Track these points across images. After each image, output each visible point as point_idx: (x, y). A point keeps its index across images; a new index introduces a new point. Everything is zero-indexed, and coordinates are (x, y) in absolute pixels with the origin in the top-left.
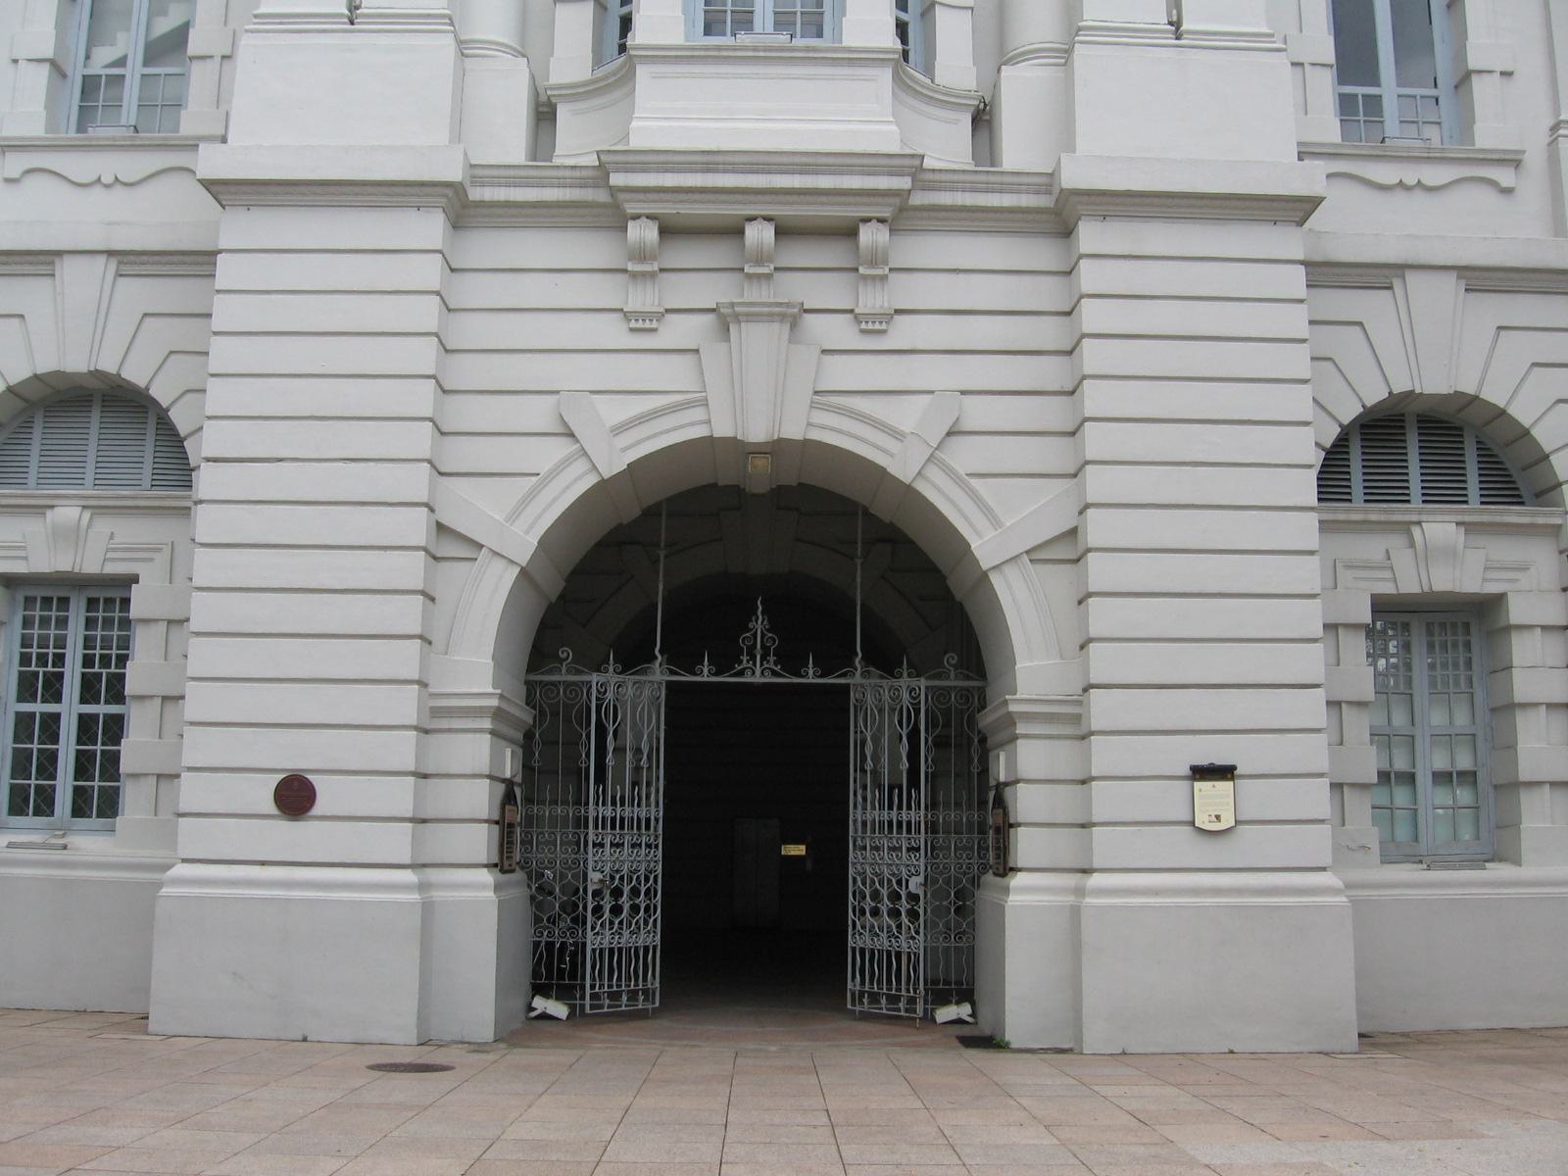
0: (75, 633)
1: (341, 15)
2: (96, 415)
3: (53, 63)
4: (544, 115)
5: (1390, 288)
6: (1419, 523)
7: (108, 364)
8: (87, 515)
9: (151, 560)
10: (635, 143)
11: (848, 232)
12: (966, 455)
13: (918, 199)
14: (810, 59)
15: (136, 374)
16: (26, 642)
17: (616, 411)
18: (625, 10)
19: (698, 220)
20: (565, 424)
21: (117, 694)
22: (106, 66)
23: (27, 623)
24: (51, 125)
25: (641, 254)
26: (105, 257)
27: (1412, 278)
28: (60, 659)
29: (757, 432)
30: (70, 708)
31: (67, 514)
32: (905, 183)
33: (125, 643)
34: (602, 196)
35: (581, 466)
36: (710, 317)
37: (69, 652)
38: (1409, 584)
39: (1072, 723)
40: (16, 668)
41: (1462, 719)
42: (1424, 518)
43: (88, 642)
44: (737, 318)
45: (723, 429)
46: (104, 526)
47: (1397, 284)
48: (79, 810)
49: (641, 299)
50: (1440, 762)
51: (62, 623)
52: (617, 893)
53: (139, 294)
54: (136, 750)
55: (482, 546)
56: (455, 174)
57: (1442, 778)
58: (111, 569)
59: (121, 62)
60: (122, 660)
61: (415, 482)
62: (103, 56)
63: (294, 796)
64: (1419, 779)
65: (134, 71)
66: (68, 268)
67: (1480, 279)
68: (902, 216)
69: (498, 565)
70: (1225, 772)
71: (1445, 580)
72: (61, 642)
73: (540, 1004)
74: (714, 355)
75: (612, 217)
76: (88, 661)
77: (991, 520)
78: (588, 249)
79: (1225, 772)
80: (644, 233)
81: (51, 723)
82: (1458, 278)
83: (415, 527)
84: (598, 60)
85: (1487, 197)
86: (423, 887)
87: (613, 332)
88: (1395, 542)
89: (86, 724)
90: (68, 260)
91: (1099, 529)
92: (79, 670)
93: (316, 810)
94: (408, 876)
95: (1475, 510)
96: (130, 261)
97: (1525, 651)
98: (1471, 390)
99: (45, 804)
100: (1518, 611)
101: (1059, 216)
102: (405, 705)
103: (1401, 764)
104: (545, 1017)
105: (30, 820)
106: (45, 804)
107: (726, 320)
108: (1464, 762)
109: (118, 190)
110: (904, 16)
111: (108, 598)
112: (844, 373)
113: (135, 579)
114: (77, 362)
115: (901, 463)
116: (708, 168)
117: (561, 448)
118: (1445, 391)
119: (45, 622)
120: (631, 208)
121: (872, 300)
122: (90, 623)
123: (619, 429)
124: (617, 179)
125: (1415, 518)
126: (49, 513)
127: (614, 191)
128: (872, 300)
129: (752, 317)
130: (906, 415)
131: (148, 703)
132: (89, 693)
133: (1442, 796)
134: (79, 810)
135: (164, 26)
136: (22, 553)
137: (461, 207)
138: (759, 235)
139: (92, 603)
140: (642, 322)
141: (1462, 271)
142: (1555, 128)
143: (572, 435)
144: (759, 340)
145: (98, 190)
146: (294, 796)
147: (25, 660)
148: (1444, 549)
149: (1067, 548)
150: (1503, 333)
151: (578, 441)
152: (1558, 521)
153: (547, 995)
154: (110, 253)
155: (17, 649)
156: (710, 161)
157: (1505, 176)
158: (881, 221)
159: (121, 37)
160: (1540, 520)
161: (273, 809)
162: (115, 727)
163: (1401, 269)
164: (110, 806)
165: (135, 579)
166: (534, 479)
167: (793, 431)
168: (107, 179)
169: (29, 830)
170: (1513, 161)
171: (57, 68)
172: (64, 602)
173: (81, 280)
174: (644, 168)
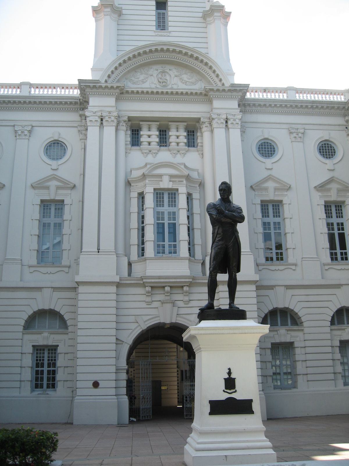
0: (46, 355)
1: (97, 251)
2: (48, 316)
3: (37, 250)
4: (130, 264)
5: (273, 289)
6: (279, 330)
7: (52, 308)
8: (49, 334)
9: (61, 342)
11: (182, 287)
13: (194, 281)
14: (175, 259)
15: (57, 309)
16: (37, 357)
17: (146, 318)
18: (143, 246)
19: (156, 286)
20: (136, 320)
21: (54, 365)
22: (44, 250)
23: (37, 353)
24: (38, 263)
25: (148, 292)
26: (51, 288)
27: (277, 287)
28: (43, 360)
29: (168, 321)
30: (46, 369)
31: (46, 334)
32: (191, 280)
33: (55, 357)
34: (141, 282)
35: (141, 329)
36: (160, 302)
37: (45, 359)
38: (278, 341)
40: (35, 362)
41: (288, 363)
42: (280, 329)
43: (49, 357)
44: (164, 303)
45: (162, 321)
46: (52, 336)
47: (274, 288)
48: (48, 387)
49: (149, 299)
50: (285, 371)
51: (44, 353)
52: (145, 399)
53: (58, 294)
54: (60, 376)
55: (123, 342)
56: (117, 279)
57: (285, 374)
58: (54, 344)
59: (48, 249)
60: (55, 360)
61: (114, 332)
62: (45, 247)
63: (96, 385)
64: (281, 374)
65: (51, 250)
66: (44, 290)
69: (126, 344)
71: (283, 340)
72: (43, 357)
73: (131, 419)
75: (144, 285)
76: (48, 360)
80: (148, 289)
81: (42, 371)
82: (285, 287)
83: (113, 339)
84: (139, 256)
85: (290, 270)
86: (117, 399)
87: (144, 305)
88: (276, 333)
89: (49, 372)
90: (44, 289)
92: (47, 362)
93: (99, 387)
94: (115, 397)
95: (290, 327)
96: (55, 289)
97: (298, 351)
98: (287, 307)
99: (42, 387)
100: (296, 345)
102: (113, 369)
103: (278, 371)
104: (132, 421)
105: (51, 389)
106: (42, 387)
107: (163, 303)
108: (289, 371)
109: (51, 275)
110: (190, 246)
111: (53, 349)
112: (182, 311)
113: (58, 346)
114: (46, 307)
116: (159, 279)
117: (137, 325)
118: (283, 307)
119: (40, 353)
120: (146, 285)
121: (186, 298)
122: (49, 353)
123: (145, 322)
124: (144, 280)
125: (278, 329)
126: (42, 334)
127: (144, 282)
128: (186, 298)
129: (166, 303)
131: (61, 368)
132: (49, 366)
133: (285, 377)
134: (48, 387)
135: (56, 241)
136: (37, 341)
137: (119, 285)
138: (167, 289)
139: (49, 350)
140: (149, 303)
141: (285, 286)
142: (302, 258)
143: (137, 322)
144: (169, 306)
145: (47, 274)
146: (96, 385)
147: (37, 360)
148: (284, 335)
150: (293, 296)
151: (139, 324)
152: (303, 329)
153: (132, 417)
154: (52, 288)
155: (35, 359)
156: (159, 277)
157: (293, 267)
158: (187, 286)
159: (48, 244)
160: (299, 329)
161: (93, 387)
162: (54, 372)
163: (275, 286)
164: (53, 386)
165: (58, 346)
166: (132, 330)
167: (174, 321)
168: (49, 272)
169: (38, 391)
171: (38, 251)
172: (44, 350)
173: (47, 293)
174: (149, 279)
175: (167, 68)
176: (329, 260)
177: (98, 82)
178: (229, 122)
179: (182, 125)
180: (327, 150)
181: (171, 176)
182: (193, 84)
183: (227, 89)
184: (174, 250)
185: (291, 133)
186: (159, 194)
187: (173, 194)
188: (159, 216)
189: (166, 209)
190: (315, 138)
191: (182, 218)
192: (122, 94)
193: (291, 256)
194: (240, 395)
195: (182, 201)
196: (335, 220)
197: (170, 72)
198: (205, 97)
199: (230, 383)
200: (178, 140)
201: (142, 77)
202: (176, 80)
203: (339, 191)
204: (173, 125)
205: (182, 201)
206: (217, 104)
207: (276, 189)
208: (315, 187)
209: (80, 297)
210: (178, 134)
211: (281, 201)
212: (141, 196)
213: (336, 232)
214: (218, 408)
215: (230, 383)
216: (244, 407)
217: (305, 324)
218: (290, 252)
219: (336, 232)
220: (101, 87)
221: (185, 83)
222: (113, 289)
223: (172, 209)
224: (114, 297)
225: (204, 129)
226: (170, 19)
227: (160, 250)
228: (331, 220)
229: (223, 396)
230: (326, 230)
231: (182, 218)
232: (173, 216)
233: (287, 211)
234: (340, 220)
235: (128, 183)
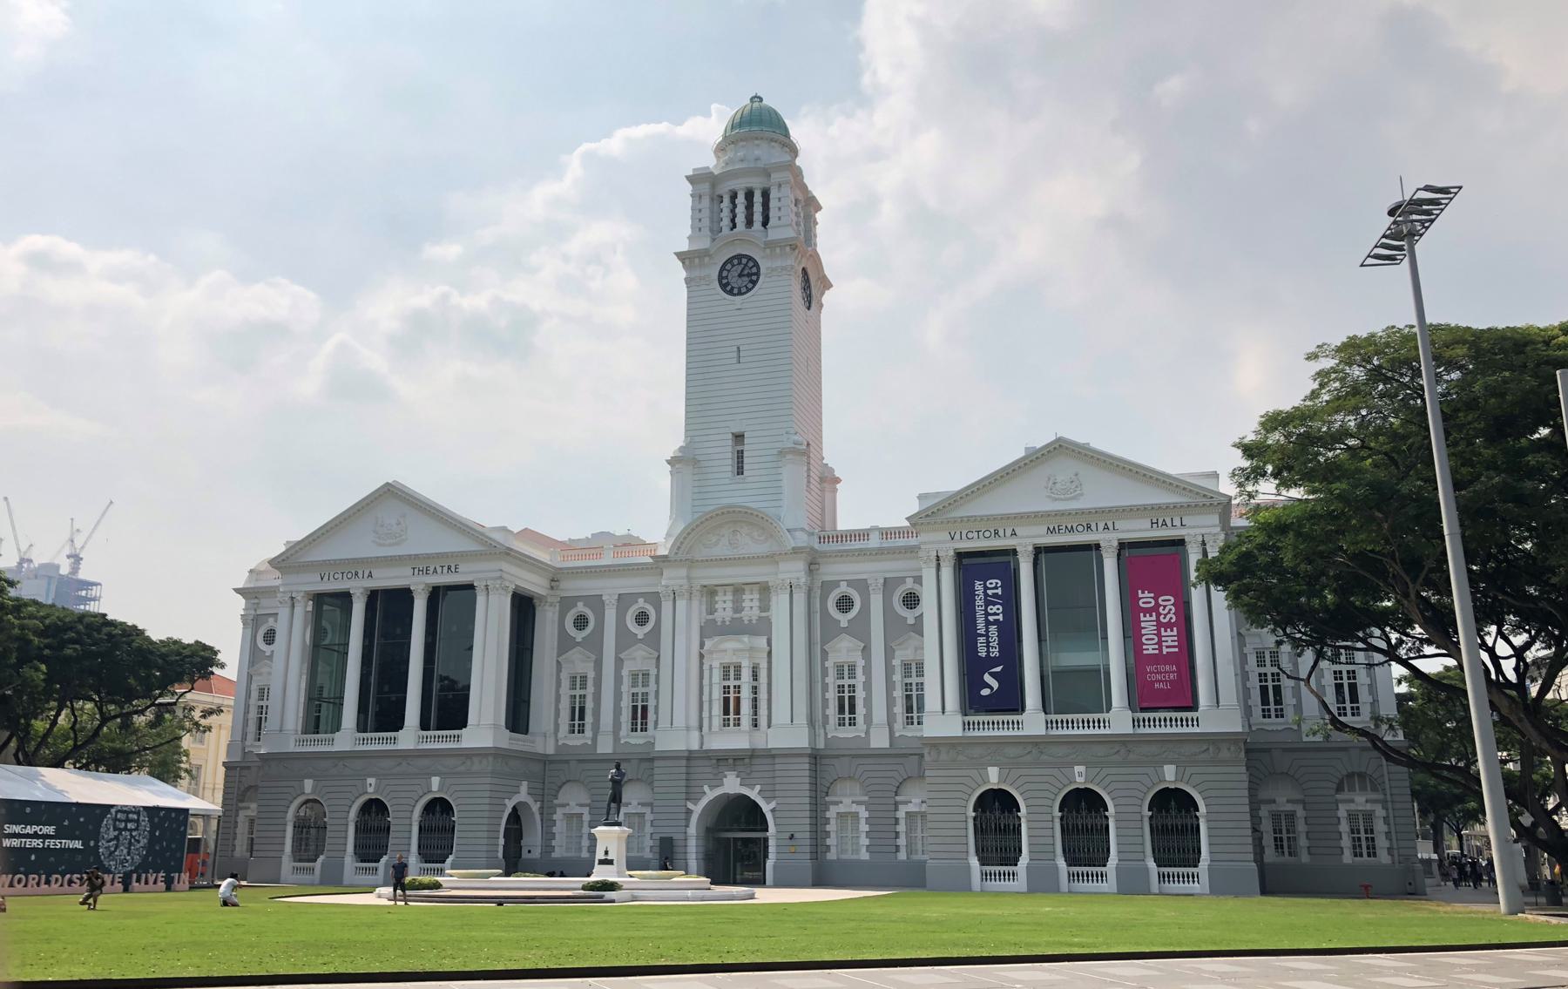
68: (751, 757)
75: (709, 758)
78: (706, 763)
101: (773, 756)
137: (688, 759)
181: (735, 651)
184: (738, 723)
186: (726, 670)
187: (738, 668)
188: (726, 689)
189: (732, 683)
191: (746, 695)
192: (691, 563)
195: (746, 675)
198: (772, 559)
205: (746, 675)
206: (782, 566)
209: (656, 771)
212: (711, 668)
214: (602, 862)
216: (610, 862)
222: (684, 762)
223: (737, 683)
224: (684, 770)
227: (726, 723)
228: (908, 680)
231: (746, 695)
232: (738, 688)
235: (702, 656)
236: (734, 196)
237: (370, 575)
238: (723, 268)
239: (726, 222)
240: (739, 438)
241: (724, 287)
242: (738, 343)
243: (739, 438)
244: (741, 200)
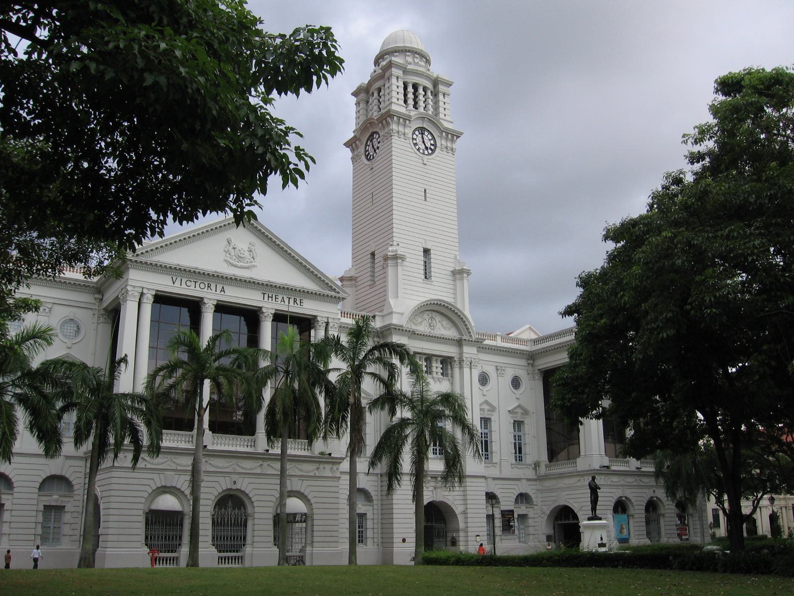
10: (430, 469)
12: (456, 502)
29: (438, 500)
39: (466, 531)
63: (404, 540)
67: (494, 479)
70: (479, 536)
74: (434, 491)
77: (458, 509)
79: (479, 536)
85: (493, 467)
91: (469, 511)
115: (450, 503)
130: (450, 498)
146: (404, 540)
149: (465, 513)
170: (496, 463)
175: (434, 314)
176: (514, 461)
177: (402, 326)
178: (472, 364)
179: (440, 359)
180: (516, 383)
182: (449, 329)
183: (474, 340)
185: (497, 370)
190: (510, 374)
193: (496, 458)
194: (604, 542)
196: (517, 433)
197: (436, 318)
198: (459, 343)
199: (602, 539)
200: (437, 371)
201: (420, 320)
202: (439, 325)
203: (522, 414)
204: (434, 358)
207: (489, 410)
208: (509, 411)
210: (437, 365)
211: (490, 419)
213: (517, 442)
215: (602, 539)
217: (501, 503)
218: (494, 454)
219: (517, 442)
220: (403, 330)
221: (445, 328)
225: (455, 366)
226: (433, 270)
229: (600, 542)
230: (513, 441)
233: (494, 426)
234: (520, 434)
236: (415, 87)
237: (223, 290)
238: (414, 133)
239: (411, 102)
240: (426, 252)
241: (415, 144)
242: (426, 187)
243: (426, 252)
244: (421, 91)
